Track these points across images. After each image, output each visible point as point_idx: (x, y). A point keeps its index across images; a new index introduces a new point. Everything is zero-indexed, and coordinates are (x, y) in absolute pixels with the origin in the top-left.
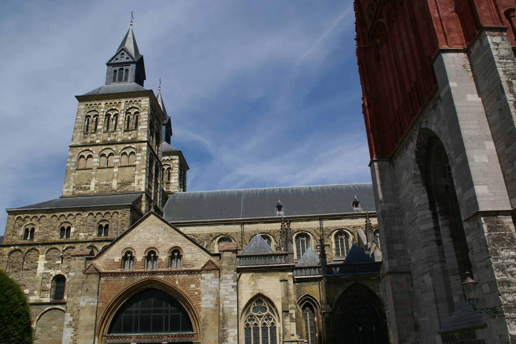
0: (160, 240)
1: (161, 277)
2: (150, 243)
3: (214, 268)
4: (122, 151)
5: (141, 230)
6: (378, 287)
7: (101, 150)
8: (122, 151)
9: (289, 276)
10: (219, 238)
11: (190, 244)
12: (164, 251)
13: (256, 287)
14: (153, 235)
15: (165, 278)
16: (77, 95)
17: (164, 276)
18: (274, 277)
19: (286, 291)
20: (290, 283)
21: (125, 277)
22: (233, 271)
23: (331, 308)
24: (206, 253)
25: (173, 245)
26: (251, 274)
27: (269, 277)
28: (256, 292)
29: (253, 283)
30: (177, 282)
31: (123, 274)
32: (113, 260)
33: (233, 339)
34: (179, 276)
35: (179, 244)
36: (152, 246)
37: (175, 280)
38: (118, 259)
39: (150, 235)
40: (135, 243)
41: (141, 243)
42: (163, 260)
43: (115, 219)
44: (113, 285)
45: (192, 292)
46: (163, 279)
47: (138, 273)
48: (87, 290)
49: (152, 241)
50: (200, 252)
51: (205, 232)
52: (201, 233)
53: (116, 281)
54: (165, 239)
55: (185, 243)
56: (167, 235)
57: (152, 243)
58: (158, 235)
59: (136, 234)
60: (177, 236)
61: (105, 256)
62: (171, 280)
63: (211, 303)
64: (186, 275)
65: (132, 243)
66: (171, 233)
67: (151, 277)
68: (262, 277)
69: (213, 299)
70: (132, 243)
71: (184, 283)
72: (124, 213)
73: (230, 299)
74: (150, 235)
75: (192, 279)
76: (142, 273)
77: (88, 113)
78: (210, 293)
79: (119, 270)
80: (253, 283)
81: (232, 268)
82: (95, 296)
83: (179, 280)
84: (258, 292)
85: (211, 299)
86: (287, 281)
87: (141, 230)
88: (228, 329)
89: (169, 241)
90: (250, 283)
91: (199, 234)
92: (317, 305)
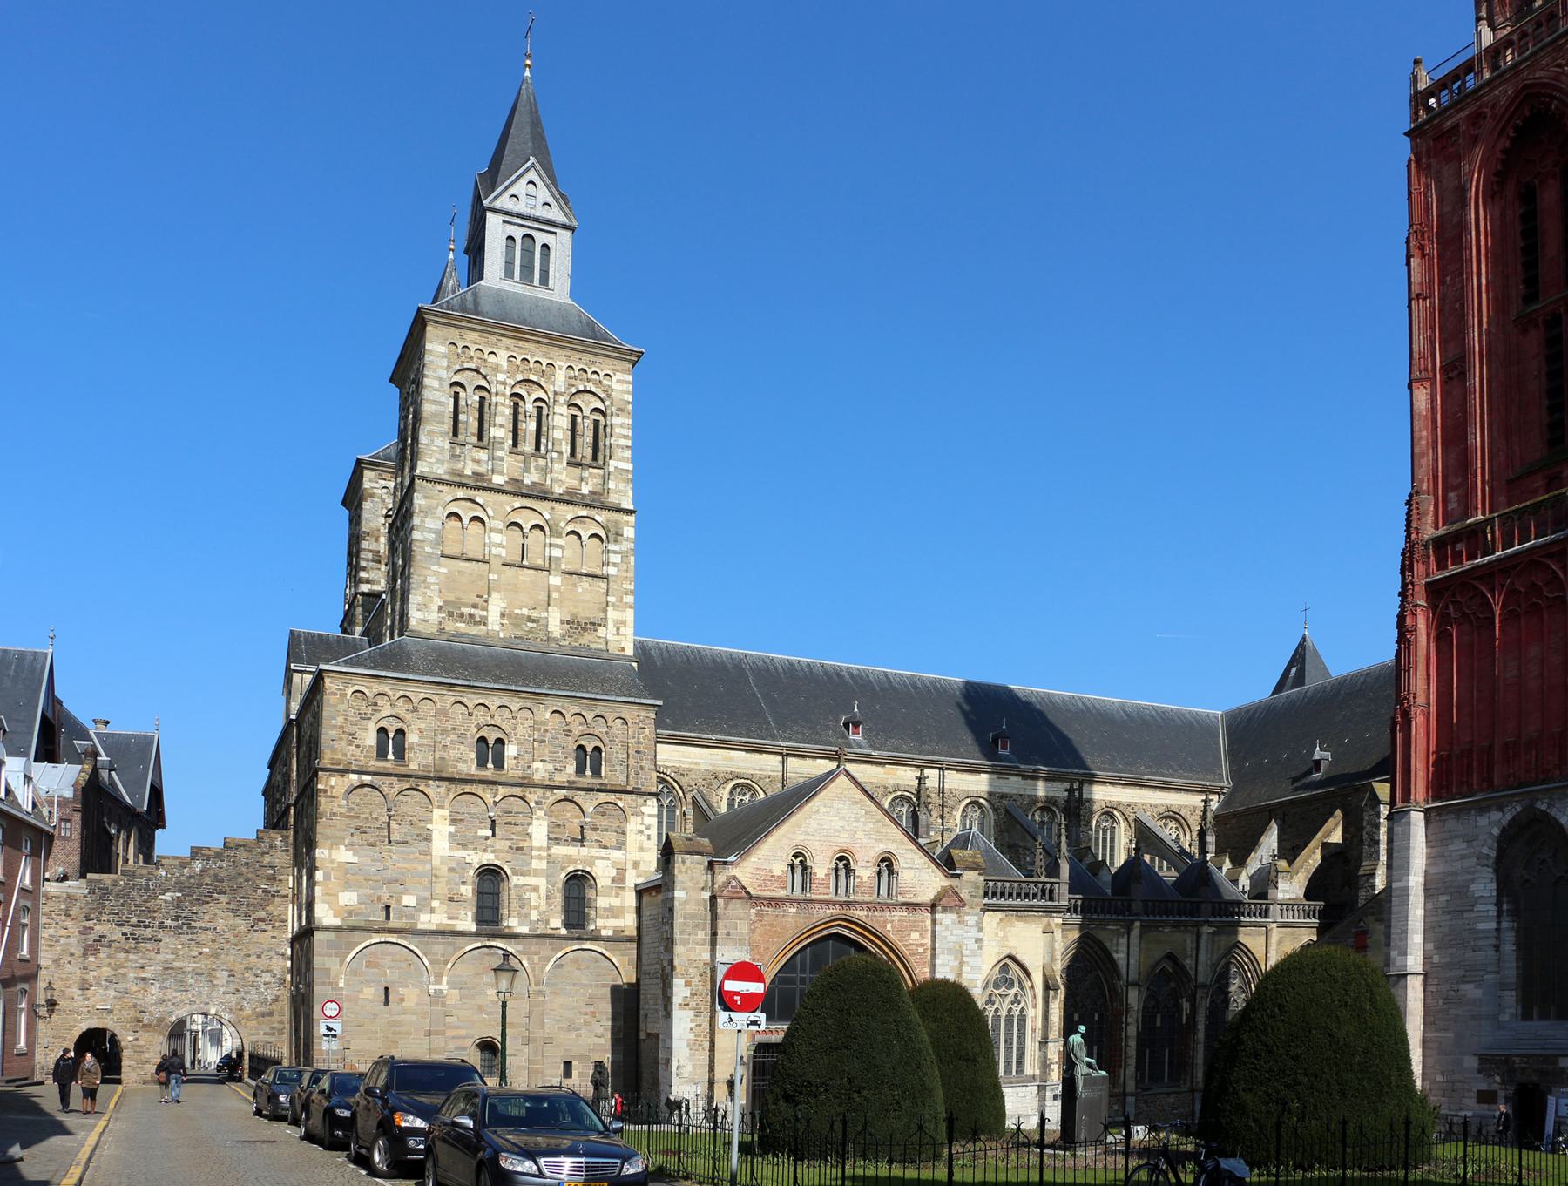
0: (860, 835)
1: (860, 914)
2: (842, 840)
3: (958, 903)
5: (823, 810)
6: (1117, 944)
9: (1057, 924)
10: (731, 784)
11: (912, 850)
12: (866, 859)
14: (846, 823)
15: (867, 916)
17: (866, 913)
21: (795, 910)
22: (977, 910)
24: (937, 870)
25: (881, 848)
26: (1000, 915)
27: (1026, 925)
29: (1001, 934)
30: (889, 927)
31: (792, 901)
32: (771, 871)
34: (893, 913)
35: (892, 848)
36: (844, 846)
37: (886, 922)
38: (780, 868)
39: (841, 823)
40: (811, 837)
41: (823, 838)
42: (865, 879)
43: (617, 737)
44: (772, 925)
45: (914, 947)
46: (864, 919)
47: (820, 902)
48: (728, 934)
49: (844, 835)
50: (929, 867)
51: (703, 767)
52: (692, 766)
53: (777, 916)
54: (867, 834)
55: (903, 847)
56: (871, 825)
57: (843, 841)
58: (854, 824)
59: (813, 817)
60: (888, 831)
61: (753, 860)
62: (878, 922)
63: (951, 971)
64: (906, 914)
65: (807, 837)
66: (878, 821)
67: (843, 912)
70: (807, 837)
71: (903, 929)
72: (641, 725)
74: (841, 823)
75: (915, 921)
76: (827, 902)
78: (950, 951)
79: (783, 893)
80: (1001, 934)
81: (977, 905)
82: (746, 948)
83: (892, 921)
85: (951, 963)
87: (823, 810)
89: (876, 840)
90: (997, 934)
91: (689, 770)
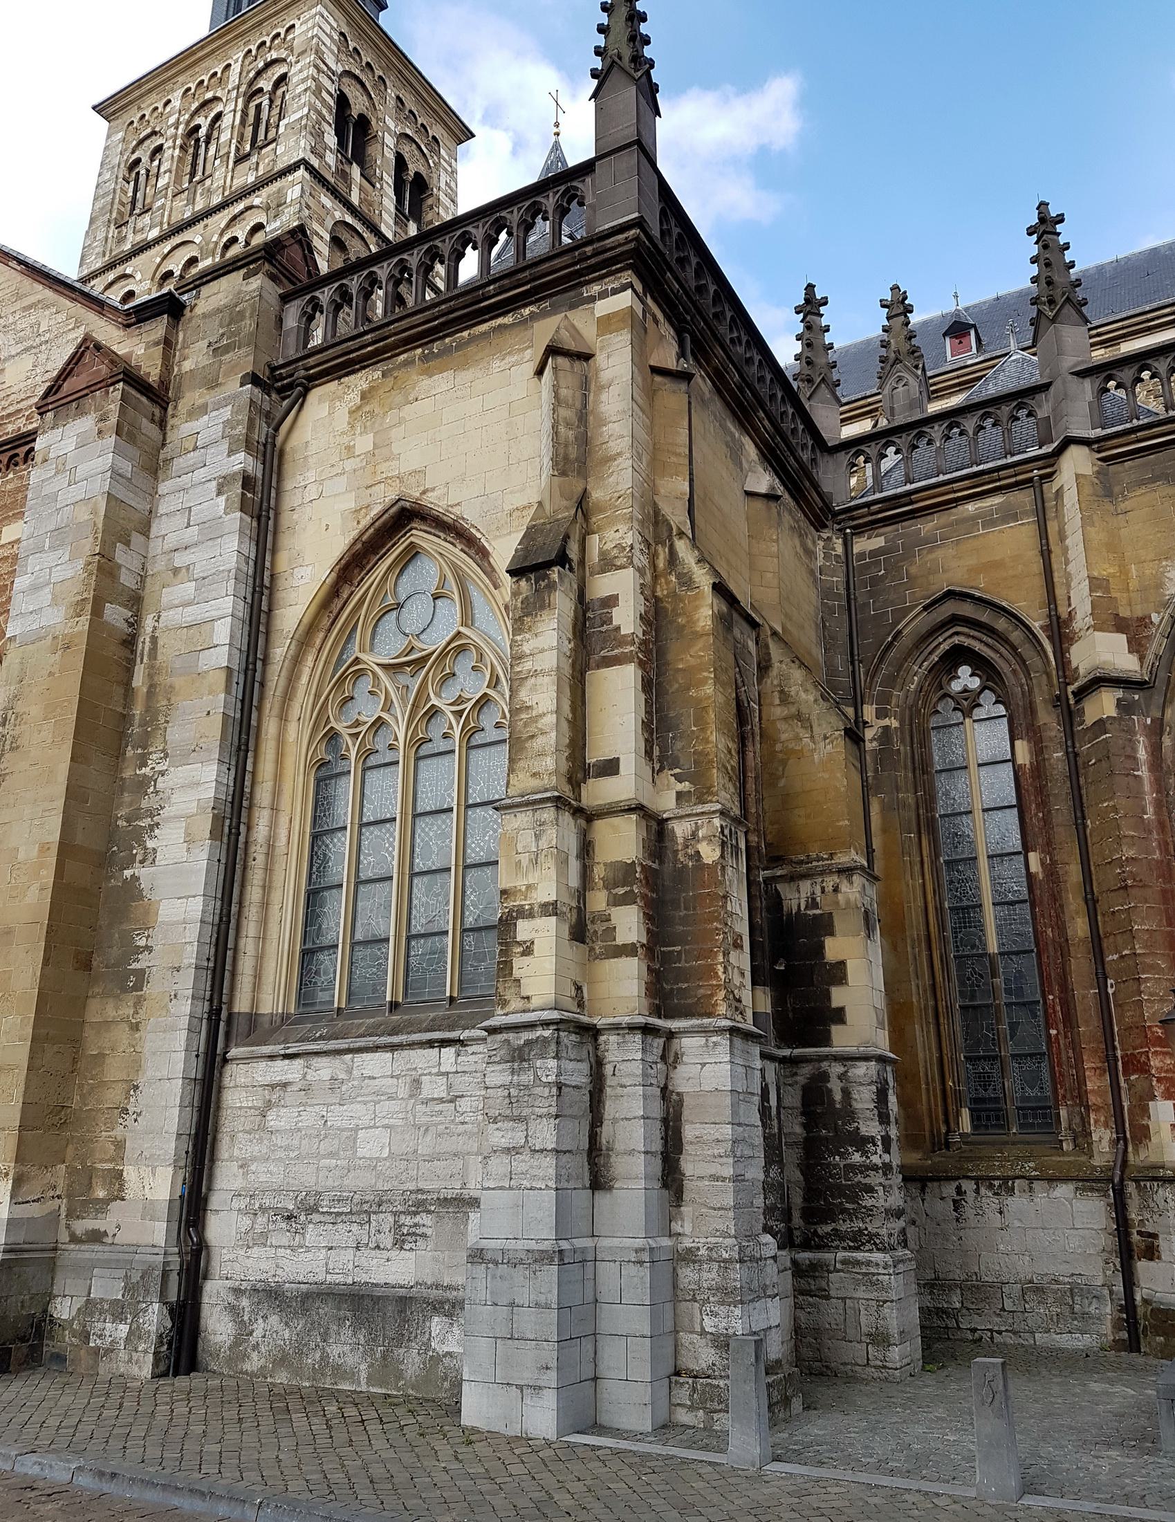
4: (221, 235)
7: (158, 260)
8: (221, 235)
13: (383, 467)
16: (96, 102)
18: (497, 365)
19: (567, 434)
20: (605, 376)
23: (1142, 659)
27: (465, 376)
28: (382, 499)
33: (187, 834)
63: (55, 602)
68: (425, 383)
69: (70, 574)
73: (198, 572)
77: (133, 152)
80: (364, 443)
84: (392, 496)
85: (57, 575)
86: (587, 357)
88: (162, 773)
92: (1026, 650)
